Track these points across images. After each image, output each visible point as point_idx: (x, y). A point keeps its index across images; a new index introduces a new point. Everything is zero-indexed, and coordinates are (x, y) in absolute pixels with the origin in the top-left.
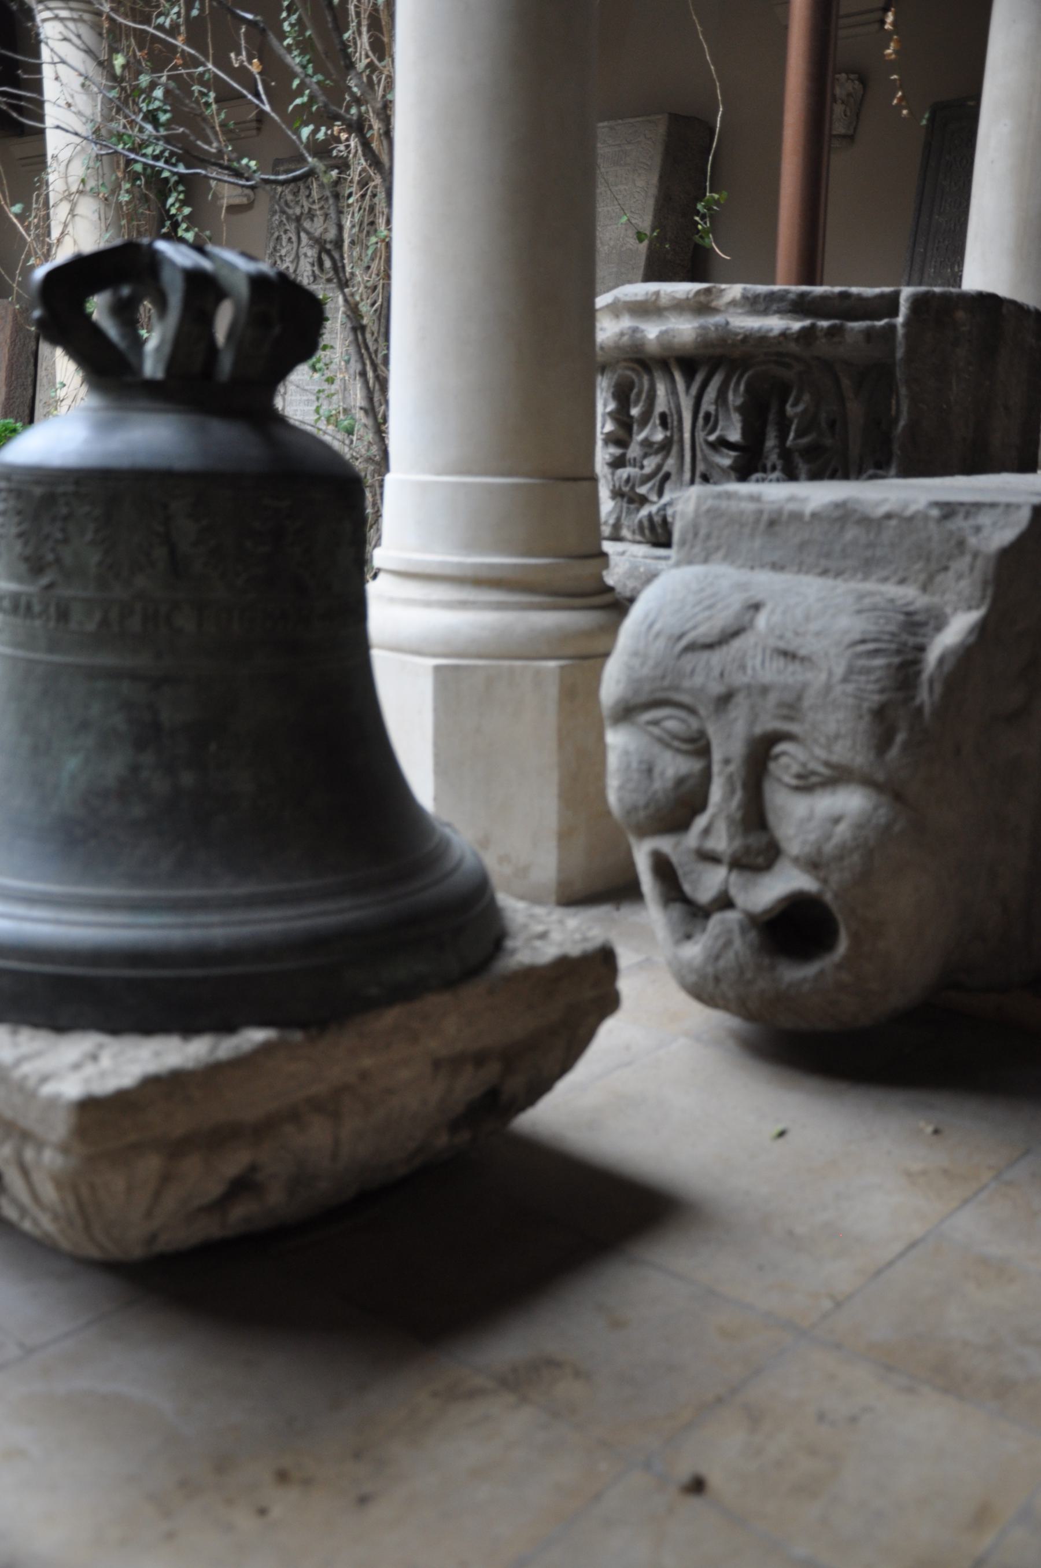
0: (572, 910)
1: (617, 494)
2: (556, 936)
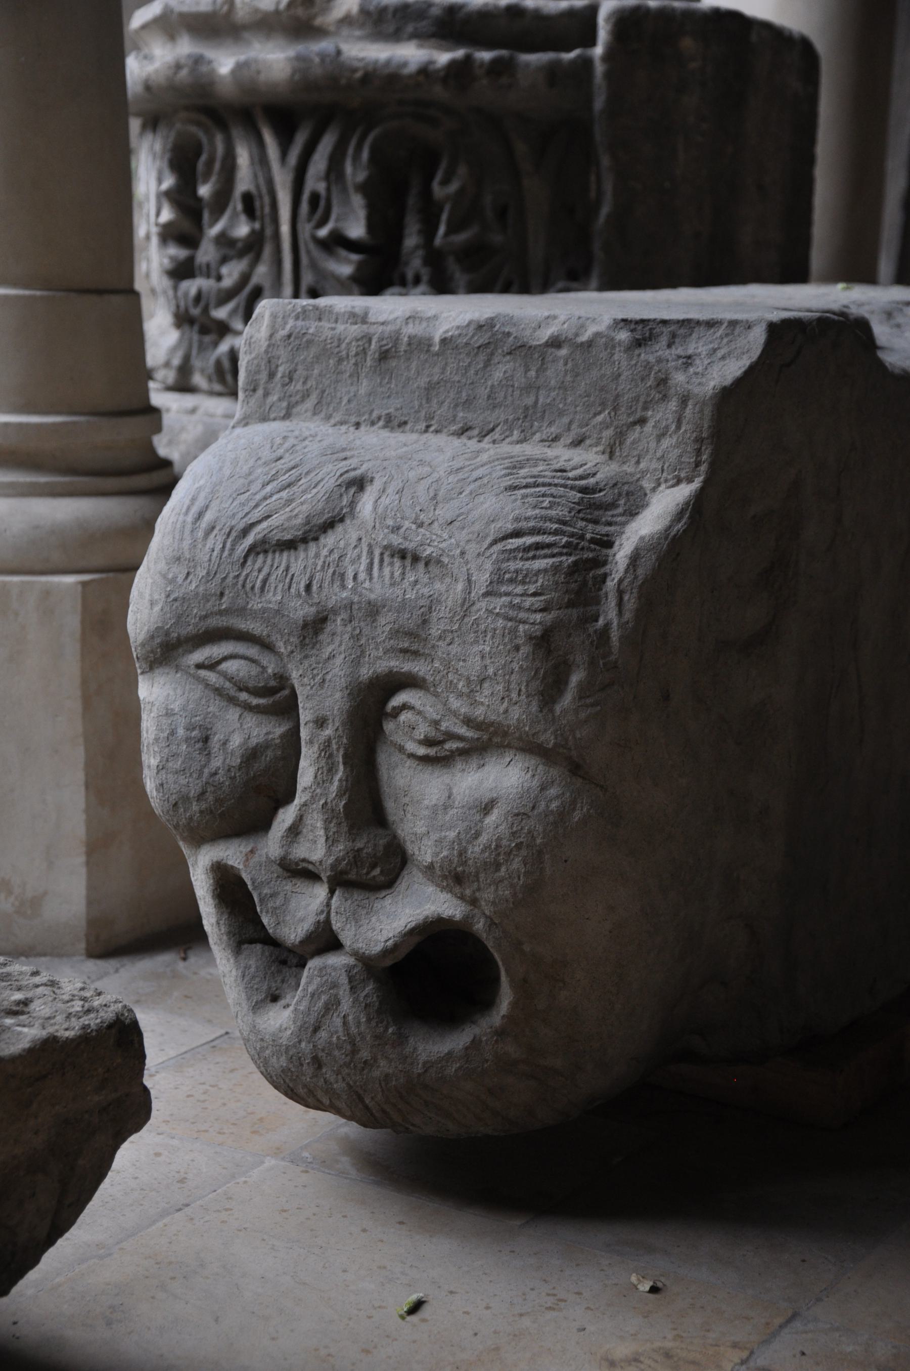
0: (110, 964)
1: (182, 319)
2: (39, 1008)
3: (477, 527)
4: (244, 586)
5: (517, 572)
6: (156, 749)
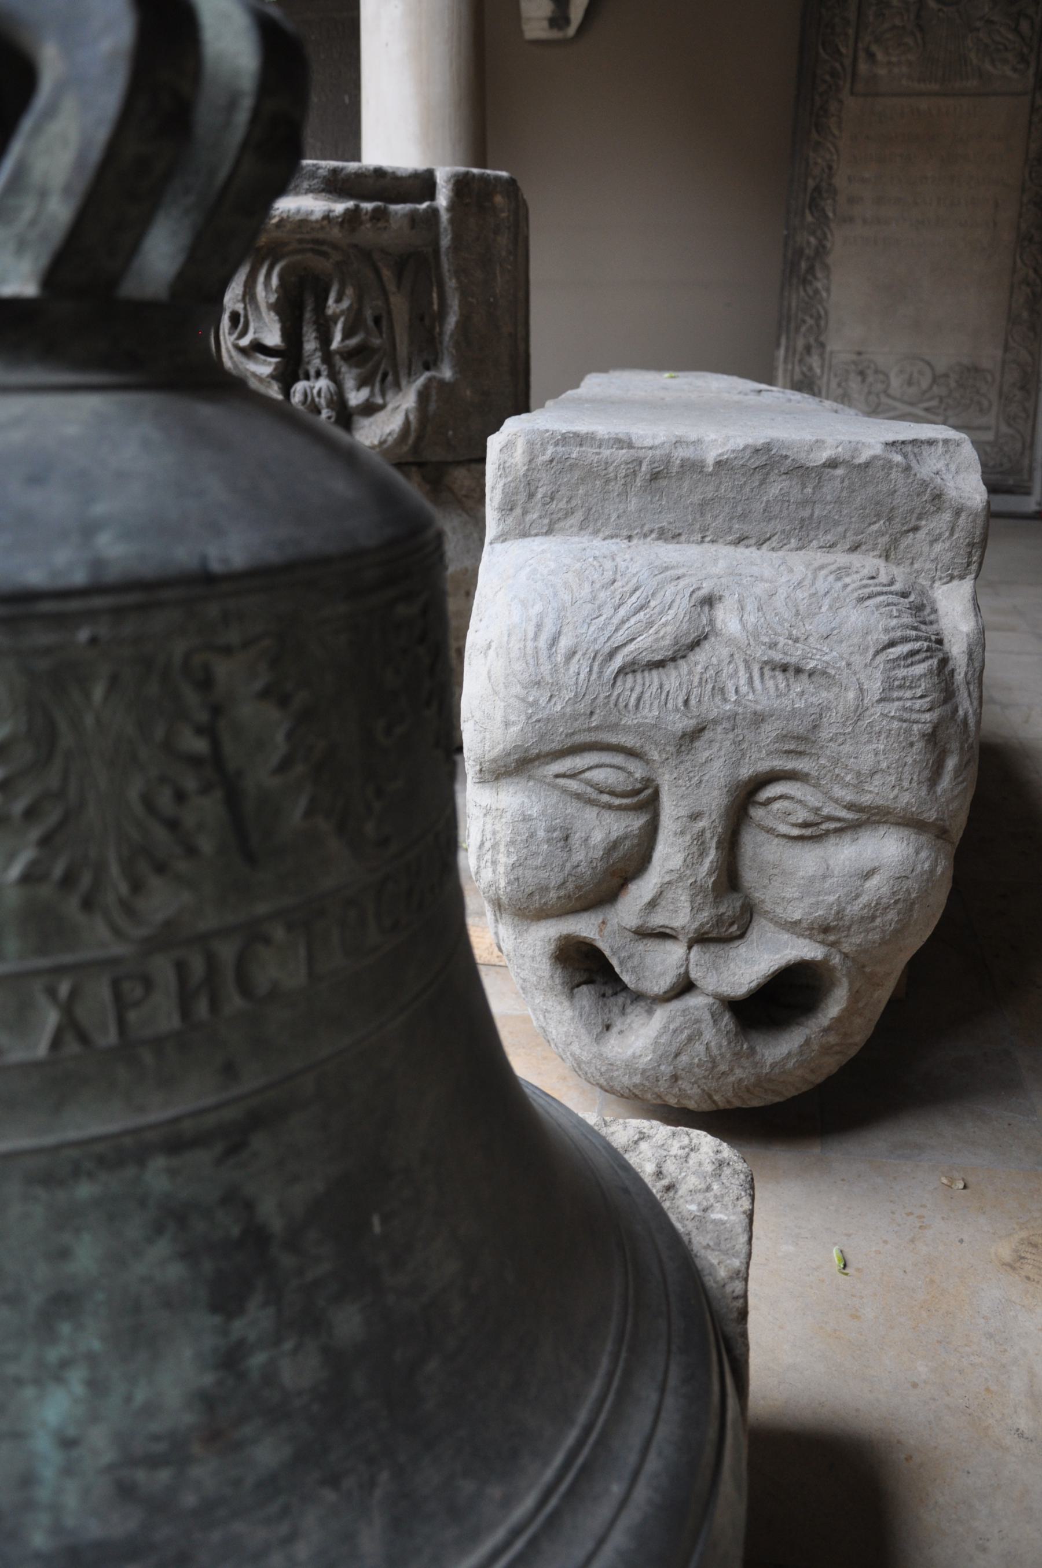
3: (856, 640)
4: (616, 705)
5: (904, 678)
6: (512, 849)
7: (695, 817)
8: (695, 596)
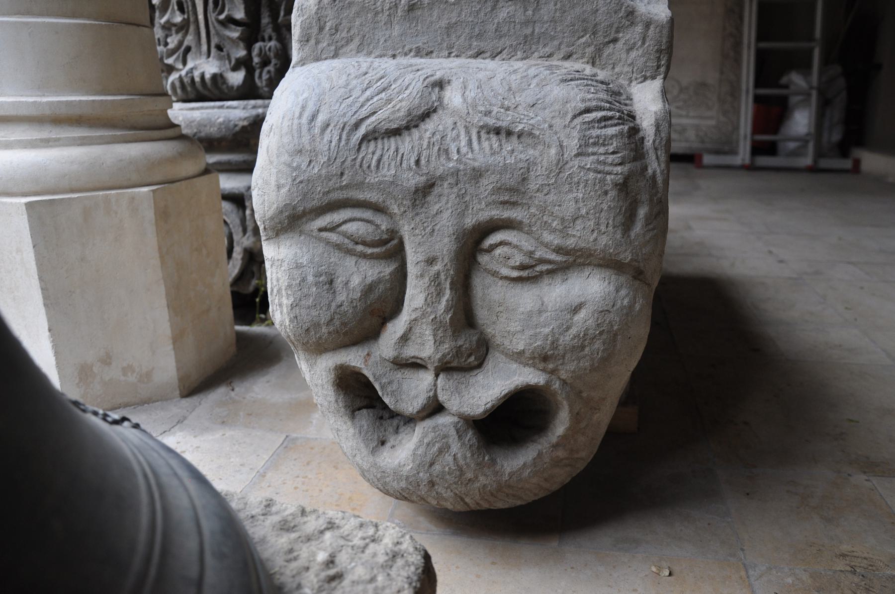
3: (556, 107)
4: (361, 166)
5: (598, 137)
6: (289, 292)
7: (431, 261)
8: (428, 80)
